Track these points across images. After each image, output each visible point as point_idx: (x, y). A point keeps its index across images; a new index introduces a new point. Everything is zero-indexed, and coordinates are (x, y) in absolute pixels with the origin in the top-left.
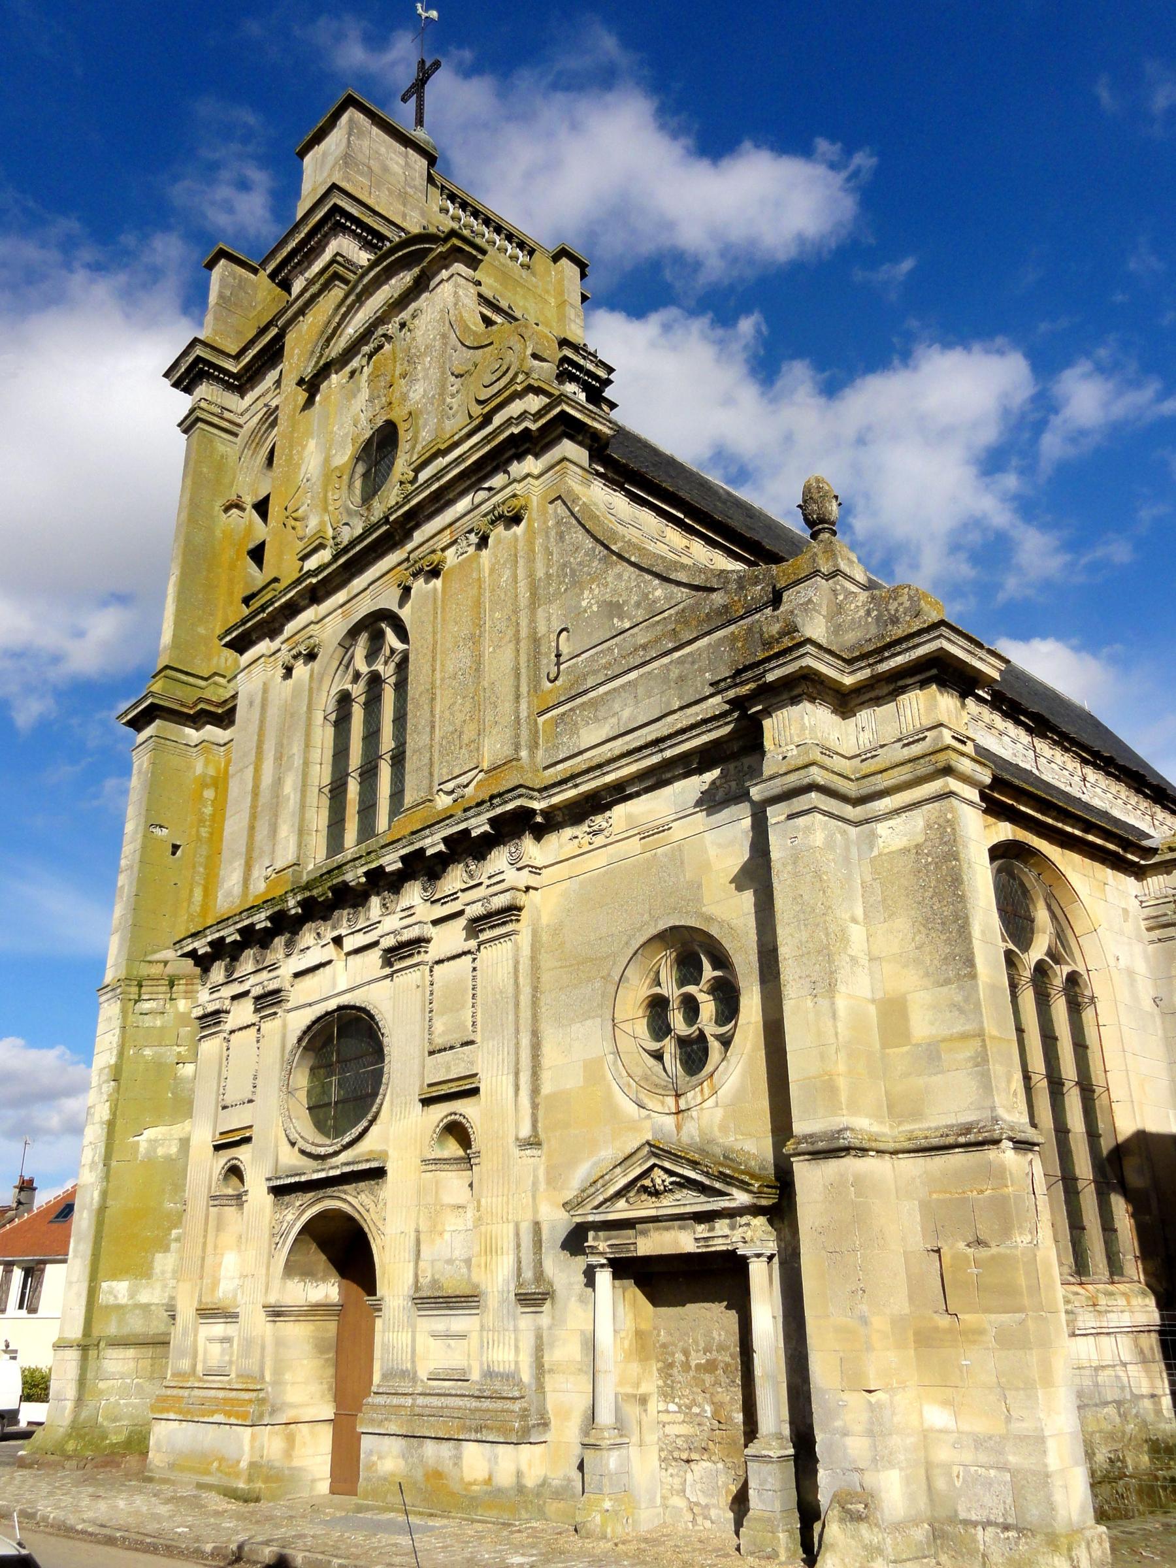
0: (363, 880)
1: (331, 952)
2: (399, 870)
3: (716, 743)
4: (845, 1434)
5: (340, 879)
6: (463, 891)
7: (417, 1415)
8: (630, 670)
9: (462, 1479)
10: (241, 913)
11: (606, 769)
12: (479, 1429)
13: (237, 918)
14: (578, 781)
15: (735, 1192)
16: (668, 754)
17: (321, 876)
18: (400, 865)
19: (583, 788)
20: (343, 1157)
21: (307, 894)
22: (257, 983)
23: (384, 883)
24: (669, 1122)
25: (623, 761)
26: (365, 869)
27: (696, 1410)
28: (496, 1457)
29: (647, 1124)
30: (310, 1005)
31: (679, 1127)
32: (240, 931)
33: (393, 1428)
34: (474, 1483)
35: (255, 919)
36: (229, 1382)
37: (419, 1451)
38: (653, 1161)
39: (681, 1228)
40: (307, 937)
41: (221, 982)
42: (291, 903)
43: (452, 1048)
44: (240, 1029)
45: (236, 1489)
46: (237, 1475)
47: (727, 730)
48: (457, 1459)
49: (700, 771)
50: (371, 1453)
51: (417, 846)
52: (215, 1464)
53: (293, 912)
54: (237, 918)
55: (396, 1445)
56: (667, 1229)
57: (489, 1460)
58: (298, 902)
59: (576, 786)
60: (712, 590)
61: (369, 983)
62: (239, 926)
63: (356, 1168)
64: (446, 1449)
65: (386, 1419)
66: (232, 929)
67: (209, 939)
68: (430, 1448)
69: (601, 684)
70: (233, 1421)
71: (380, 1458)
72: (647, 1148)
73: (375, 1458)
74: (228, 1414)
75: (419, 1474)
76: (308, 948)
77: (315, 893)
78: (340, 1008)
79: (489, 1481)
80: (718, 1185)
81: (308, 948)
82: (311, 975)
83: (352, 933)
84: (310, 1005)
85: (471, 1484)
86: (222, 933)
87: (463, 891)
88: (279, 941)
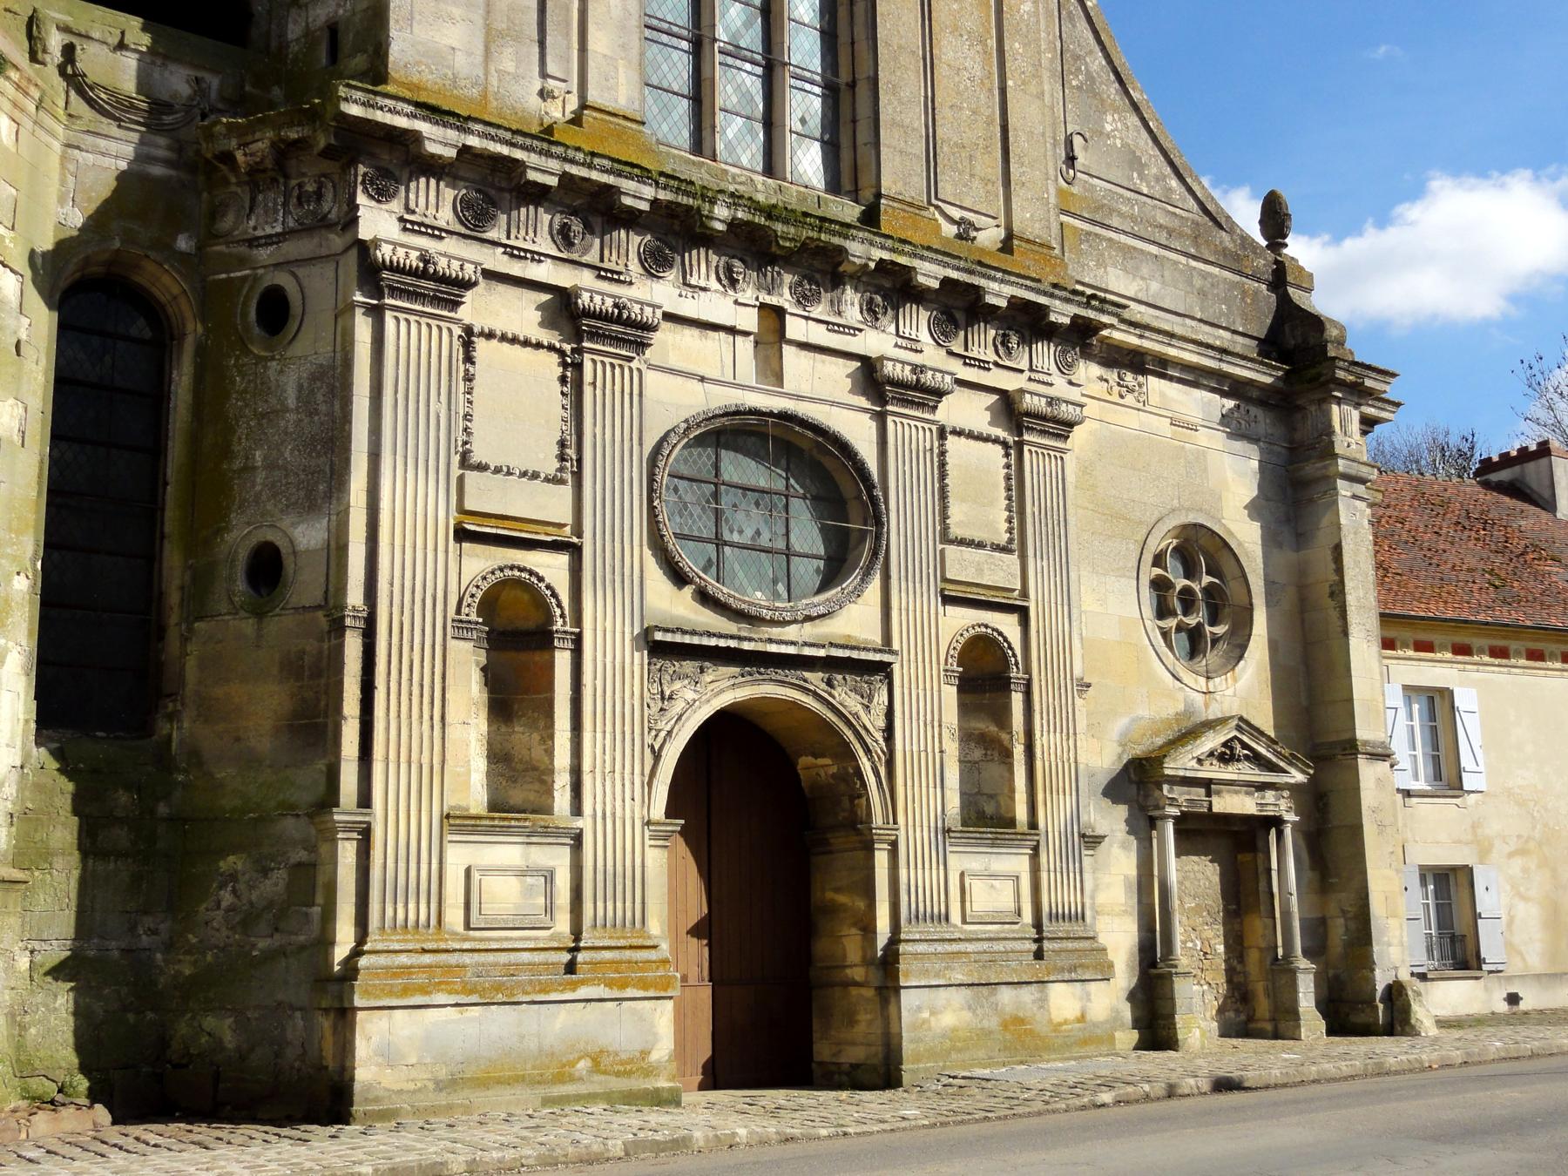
0: (872, 265)
1: (749, 320)
2: (929, 289)
3: (1251, 382)
4: (1389, 945)
5: (836, 240)
6: (996, 364)
7: (992, 960)
8: (1154, 243)
9: (1050, 1021)
10: (593, 154)
11: (1174, 342)
12: (1073, 969)
13: (580, 156)
14: (1147, 334)
15: (1293, 771)
16: (1226, 368)
17: (806, 214)
18: (935, 285)
19: (1146, 344)
20: (791, 632)
21: (760, 220)
22: (594, 292)
23: (893, 289)
24: (1199, 699)
25: (1191, 347)
26: (886, 256)
27: (1190, 945)
28: (1088, 994)
29: (1180, 696)
30: (702, 379)
31: (1207, 706)
32: (565, 178)
33: (959, 977)
34: (1066, 1022)
35: (627, 185)
36: (552, 938)
37: (992, 999)
38: (1235, 733)
39: (1247, 793)
40: (704, 266)
41: (442, 223)
42: (721, 212)
43: (980, 545)
44: (503, 338)
45: (657, 1090)
46: (649, 1072)
47: (1269, 380)
48: (1043, 1002)
49: (1224, 394)
50: (919, 1009)
51: (976, 281)
52: (583, 1065)
53: (720, 227)
54: (580, 156)
55: (959, 997)
56: (1237, 792)
57: (1081, 999)
58: (734, 219)
59: (1141, 337)
60: (1221, 228)
61: (833, 403)
62: (574, 170)
63: (855, 655)
64: (1027, 995)
65: (946, 968)
66: (554, 165)
67: (473, 141)
68: (1006, 995)
69: (1125, 232)
70: (630, 993)
71: (933, 1013)
72: (1235, 722)
73: (926, 1015)
74: (610, 984)
75: (993, 1023)
76: (704, 289)
77: (779, 227)
78: (785, 416)
79: (1082, 1018)
80: (1282, 764)
81: (704, 289)
82: (695, 332)
83: (807, 318)
84: (702, 379)
85: (1060, 1024)
86: (519, 154)
87: (996, 364)
88: (635, 242)
